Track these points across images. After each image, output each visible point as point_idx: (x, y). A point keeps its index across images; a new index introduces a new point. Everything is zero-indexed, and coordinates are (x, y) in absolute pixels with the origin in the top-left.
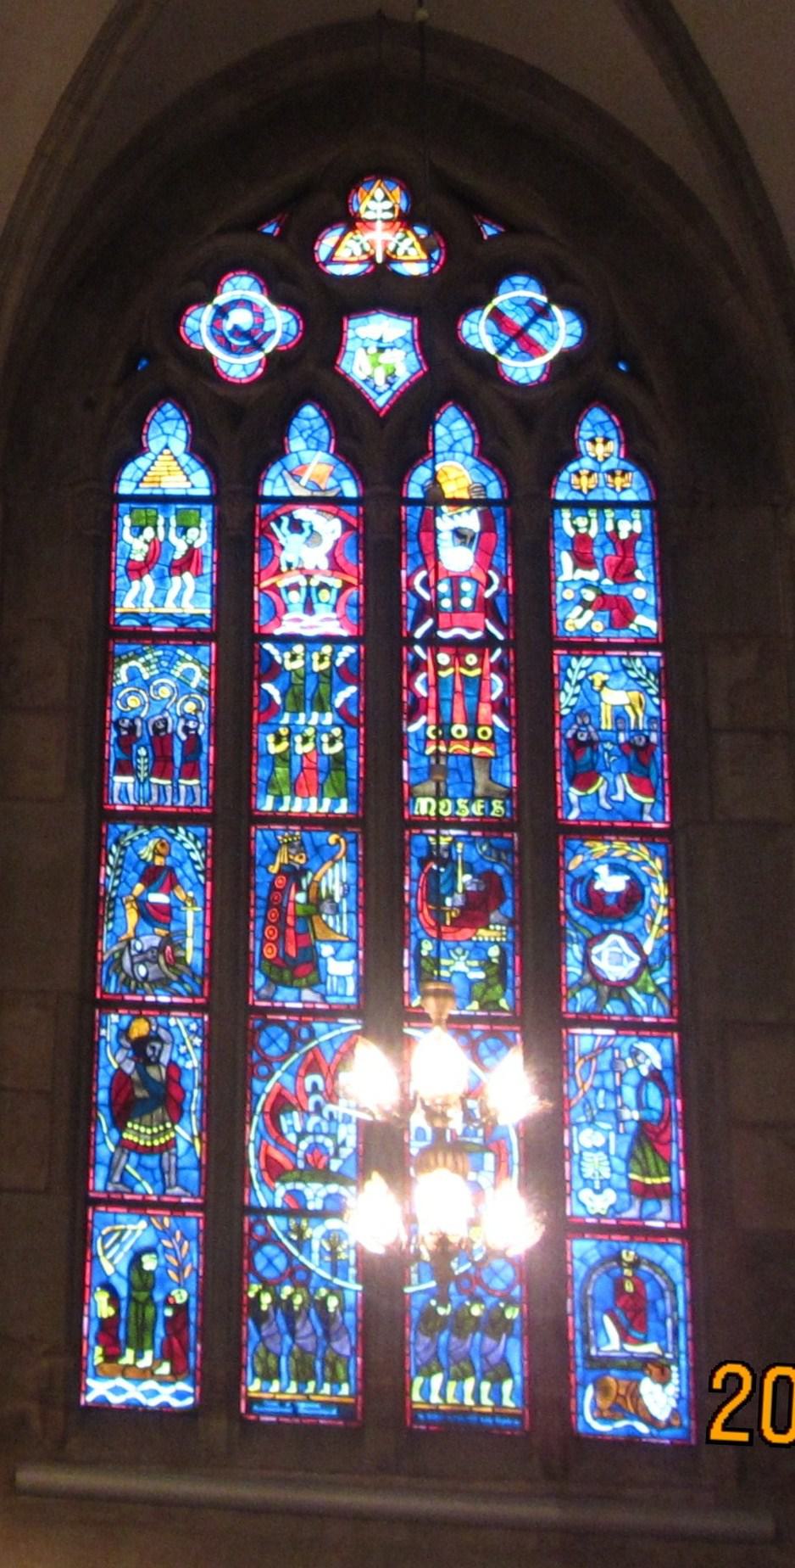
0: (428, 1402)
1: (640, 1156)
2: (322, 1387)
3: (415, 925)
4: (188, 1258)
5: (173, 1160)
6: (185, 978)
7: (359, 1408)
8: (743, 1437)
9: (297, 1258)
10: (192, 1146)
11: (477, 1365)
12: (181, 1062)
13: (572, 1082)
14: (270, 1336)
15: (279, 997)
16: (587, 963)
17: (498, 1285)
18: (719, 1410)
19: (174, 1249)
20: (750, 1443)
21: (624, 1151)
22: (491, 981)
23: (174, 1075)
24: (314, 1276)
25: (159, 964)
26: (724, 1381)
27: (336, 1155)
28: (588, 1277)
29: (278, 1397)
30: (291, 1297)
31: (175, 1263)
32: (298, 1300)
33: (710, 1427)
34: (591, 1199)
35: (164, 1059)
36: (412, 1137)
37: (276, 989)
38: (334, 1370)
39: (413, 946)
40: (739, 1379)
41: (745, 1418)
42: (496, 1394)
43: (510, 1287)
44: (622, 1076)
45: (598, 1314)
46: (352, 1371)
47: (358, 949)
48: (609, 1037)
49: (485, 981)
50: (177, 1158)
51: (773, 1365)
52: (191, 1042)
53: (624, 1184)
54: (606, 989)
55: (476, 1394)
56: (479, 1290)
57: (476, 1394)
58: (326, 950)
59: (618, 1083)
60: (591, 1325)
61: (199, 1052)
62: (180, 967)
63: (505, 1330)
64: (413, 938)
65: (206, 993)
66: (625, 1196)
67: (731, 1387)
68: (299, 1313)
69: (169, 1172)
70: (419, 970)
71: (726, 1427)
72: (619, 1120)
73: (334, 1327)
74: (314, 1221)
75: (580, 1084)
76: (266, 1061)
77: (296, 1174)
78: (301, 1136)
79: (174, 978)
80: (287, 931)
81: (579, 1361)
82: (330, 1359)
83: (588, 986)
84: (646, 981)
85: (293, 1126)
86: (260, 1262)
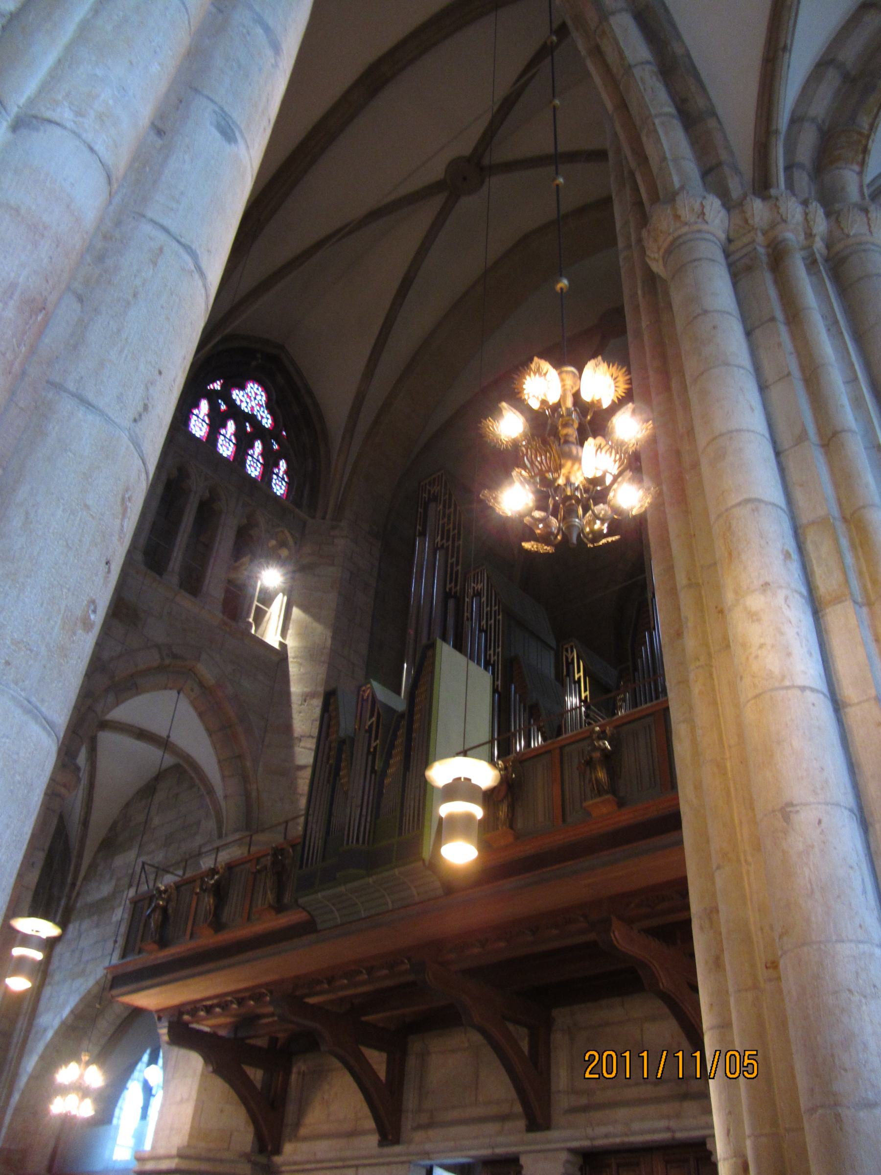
8: (597, 1076)
18: (588, 1067)
20: (599, 1078)
26: (589, 1057)
33: (585, 1073)
40: (595, 1056)
41: (597, 1070)
51: (605, 1051)
67: (592, 1057)
71: (590, 1073)
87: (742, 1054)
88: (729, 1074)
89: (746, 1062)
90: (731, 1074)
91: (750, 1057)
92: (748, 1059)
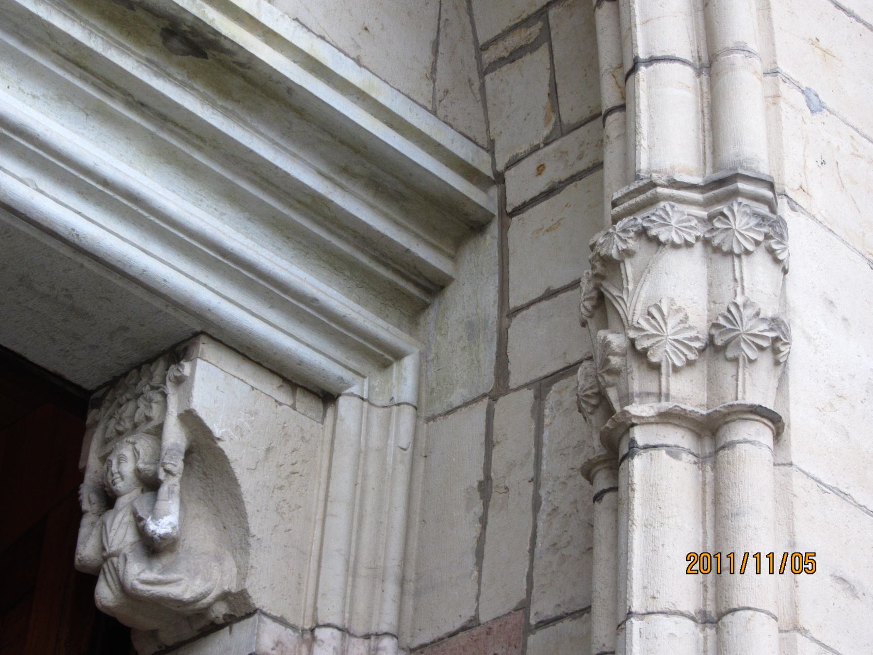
87: (804, 556)
88: (794, 571)
89: (807, 561)
90: (796, 570)
91: (810, 558)
92: (809, 559)
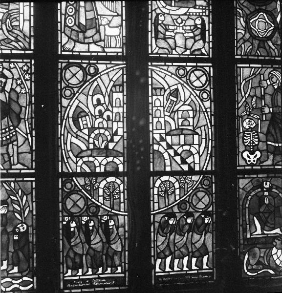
0: (164, 272)
1: (273, 131)
2: (107, 270)
3: (155, 5)
4: (27, 205)
5: (15, 148)
6: (19, 38)
7: (127, 279)
9: (90, 200)
10: (27, 139)
11: (190, 249)
12: (18, 89)
13: (240, 95)
14: (75, 245)
15: (76, 49)
16: (247, 28)
17: (201, 206)
19: (18, 201)
21: (265, 130)
22: (197, 38)
23: (14, 96)
24: (101, 209)
25: (3, 31)
27: (112, 140)
28: (246, 197)
29: (81, 277)
30: (88, 222)
31: (19, 209)
32: (92, 224)
34: (248, 156)
35: (8, 88)
36: (155, 128)
37: (75, 45)
38: (112, 259)
39: (153, 18)
42: (200, 264)
43: (207, 206)
44: (265, 89)
45: (251, 216)
46: (123, 261)
47: (122, 20)
48: (259, 68)
49: (193, 38)
50: (18, 147)
52: (24, 77)
53: (265, 148)
54: (257, 42)
55: (189, 264)
56: (191, 210)
57: (189, 264)
58: (104, 21)
59: (263, 94)
60: (248, 223)
61: (28, 83)
62: (16, 31)
63: (204, 229)
64: (154, 12)
65: (32, 48)
66: (265, 153)
68: (93, 230)
69: (13, 156)
70: (157, 32)
72: (263, 113)
73: (113, 237)
74: (99, 179)
75: (243, 94)
76: (71, 87)
77: (89, 152)
78: (92, 129)
79: (13, 39)
80: (80, 8)
81: (242, 242)
82: (111, 255)
83: (248, 40)
84: (277, 37)
85: (87, 124)
86: (69, 204)
